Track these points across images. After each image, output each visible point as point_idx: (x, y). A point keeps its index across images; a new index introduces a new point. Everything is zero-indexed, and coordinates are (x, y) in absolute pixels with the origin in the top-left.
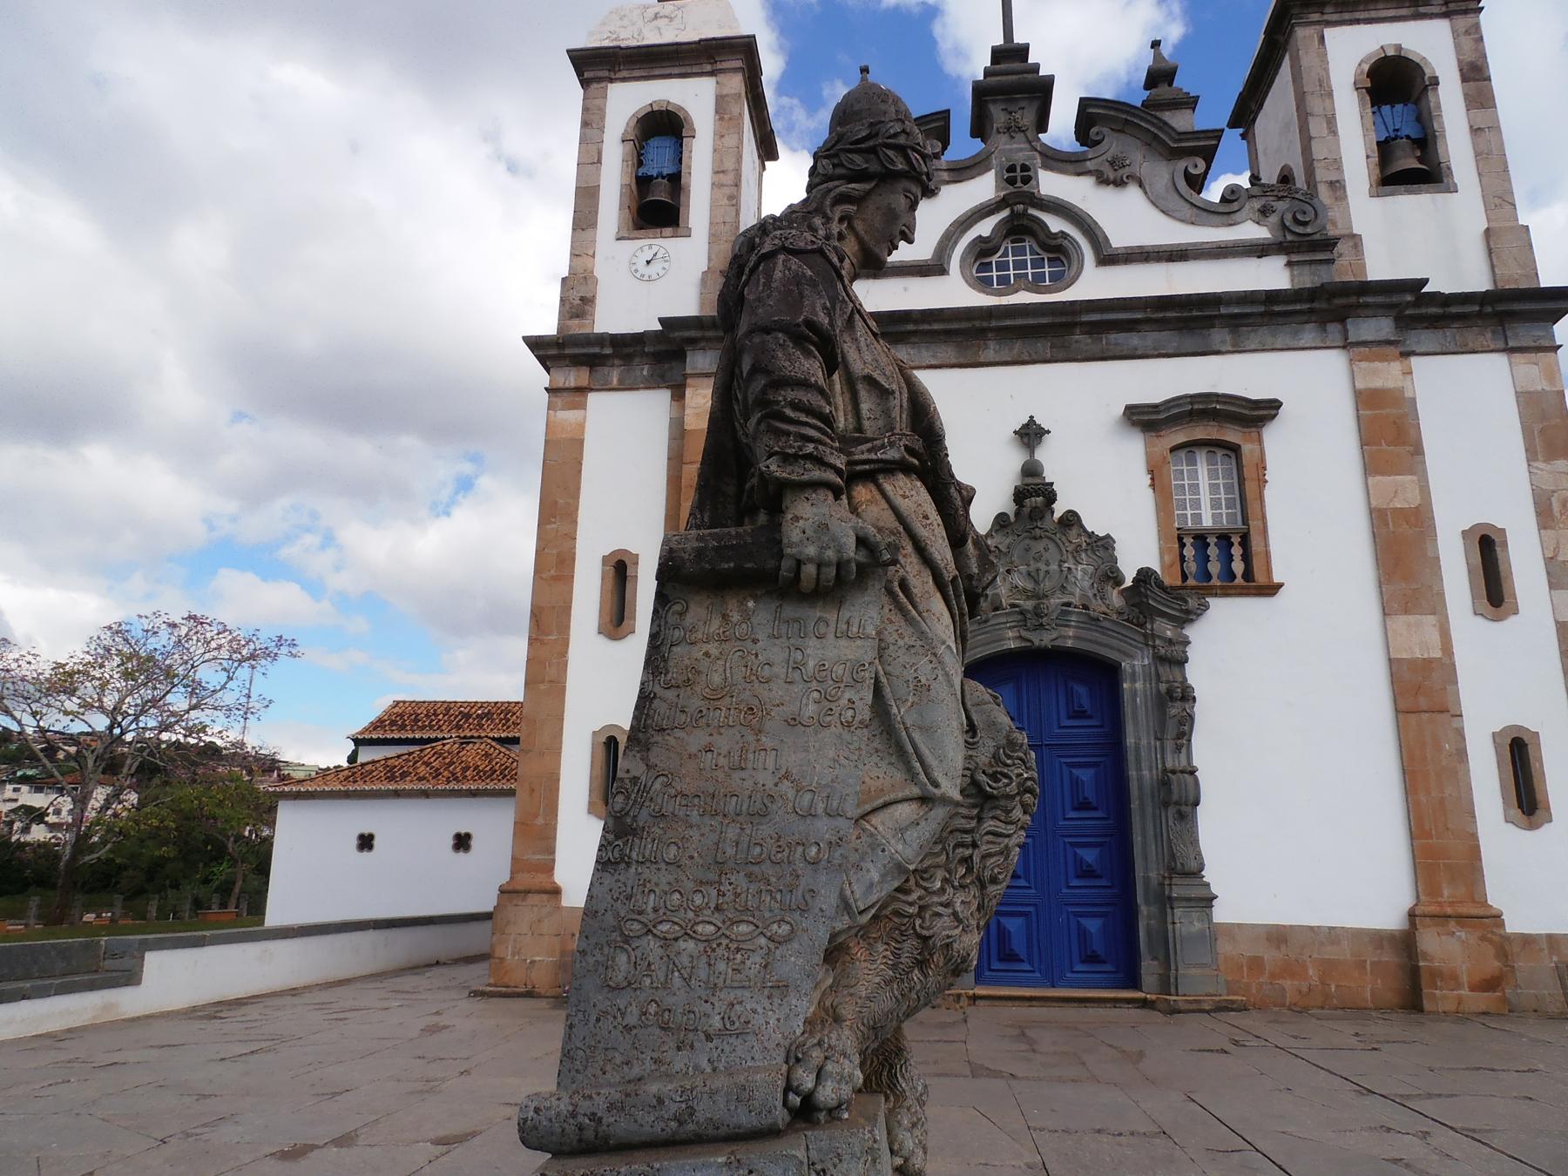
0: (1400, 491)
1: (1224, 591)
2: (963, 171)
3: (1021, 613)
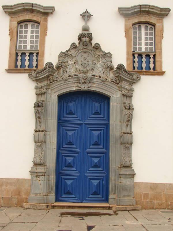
1: (146, 73)
3: (78, 78)
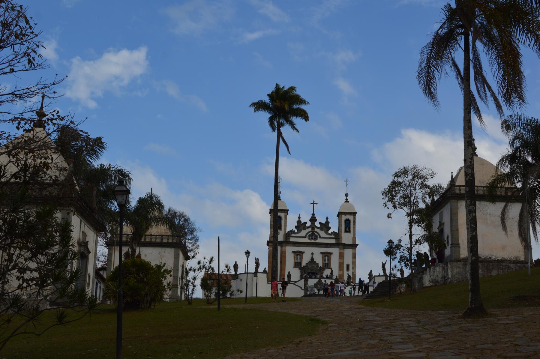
0: (342, 261)
2: (308, 227)
